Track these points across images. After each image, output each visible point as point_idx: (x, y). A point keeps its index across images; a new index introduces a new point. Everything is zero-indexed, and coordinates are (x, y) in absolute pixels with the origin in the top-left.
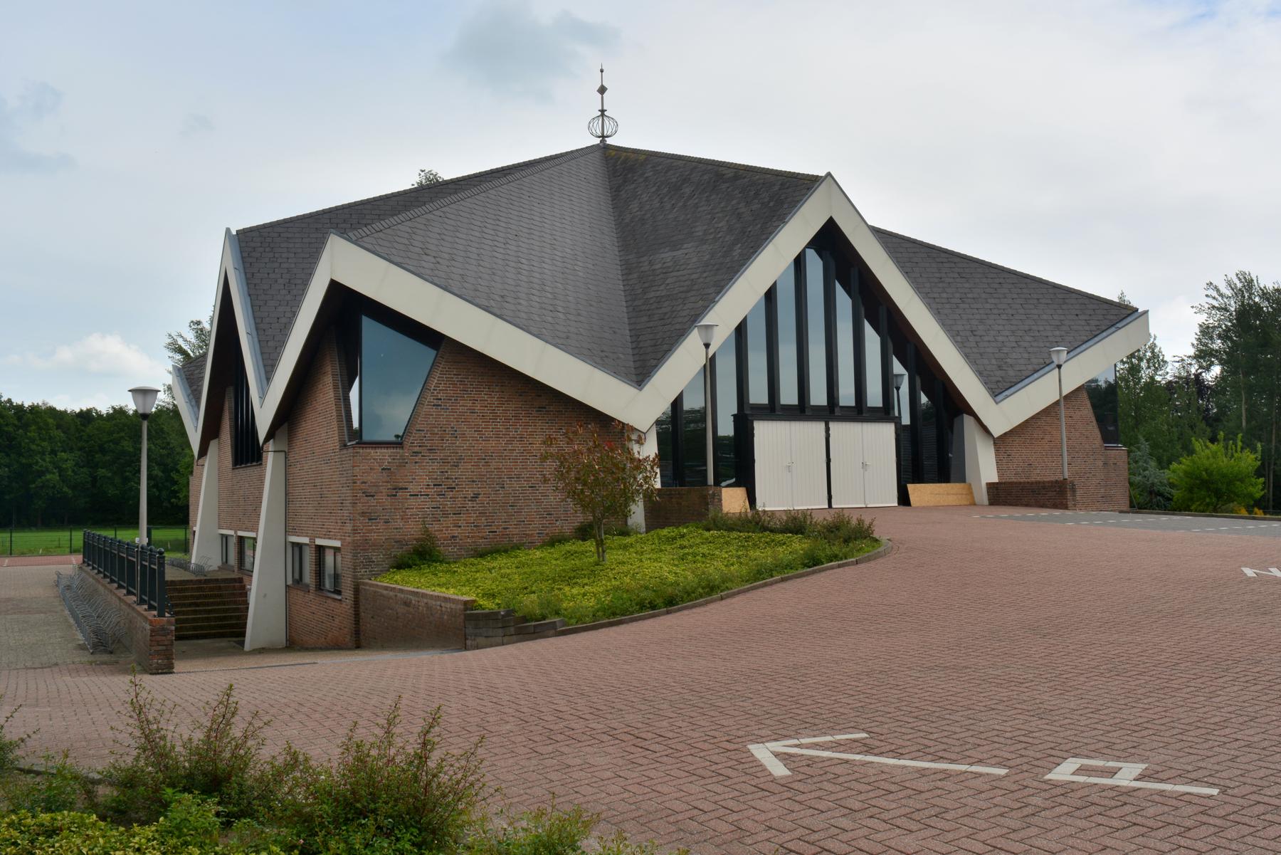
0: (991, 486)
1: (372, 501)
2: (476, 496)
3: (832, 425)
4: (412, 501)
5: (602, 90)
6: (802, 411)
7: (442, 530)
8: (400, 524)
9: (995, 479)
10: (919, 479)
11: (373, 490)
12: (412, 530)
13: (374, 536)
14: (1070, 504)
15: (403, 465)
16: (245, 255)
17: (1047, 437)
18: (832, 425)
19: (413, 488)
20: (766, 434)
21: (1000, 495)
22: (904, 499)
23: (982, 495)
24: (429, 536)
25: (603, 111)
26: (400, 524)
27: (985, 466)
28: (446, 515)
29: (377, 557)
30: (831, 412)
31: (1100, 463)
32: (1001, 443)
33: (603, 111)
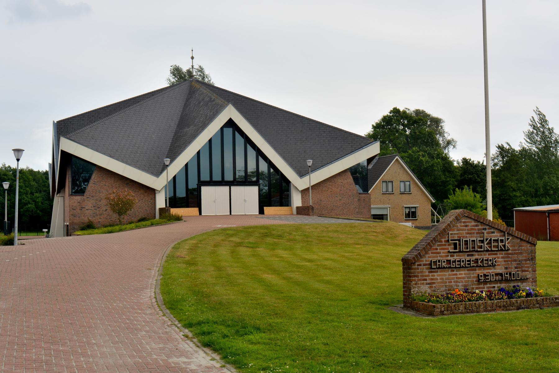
0: (297, 208)
1: (75, 211)
2: (106, 210)
3: (232, 187)
4: (87, 211)
5: (192, 58)
6: (222, 183)
7: (95, 220)
8: (83, 218)
9: (301, 205)
10: (270, 205)
11: (75, 208)
12: (86, 220)
13: (75, 221)
14: (311, 214)
15: (84, 201)
16: (70, 120)
17: (330, 190)
18: (232, 187)
19: (87, 208)
20: (205, 191)
21: (301, 211)
22: (261, 212)
23: (295, 211)
24: (90, 221)
25: (193, 66)
26: (83, 218)
27: (297, 201)
28: (97, 215)
29: (76, 227)
30: (230, 184)
31: (357, 200)
32: (305, 192)
33: (193, 66)
